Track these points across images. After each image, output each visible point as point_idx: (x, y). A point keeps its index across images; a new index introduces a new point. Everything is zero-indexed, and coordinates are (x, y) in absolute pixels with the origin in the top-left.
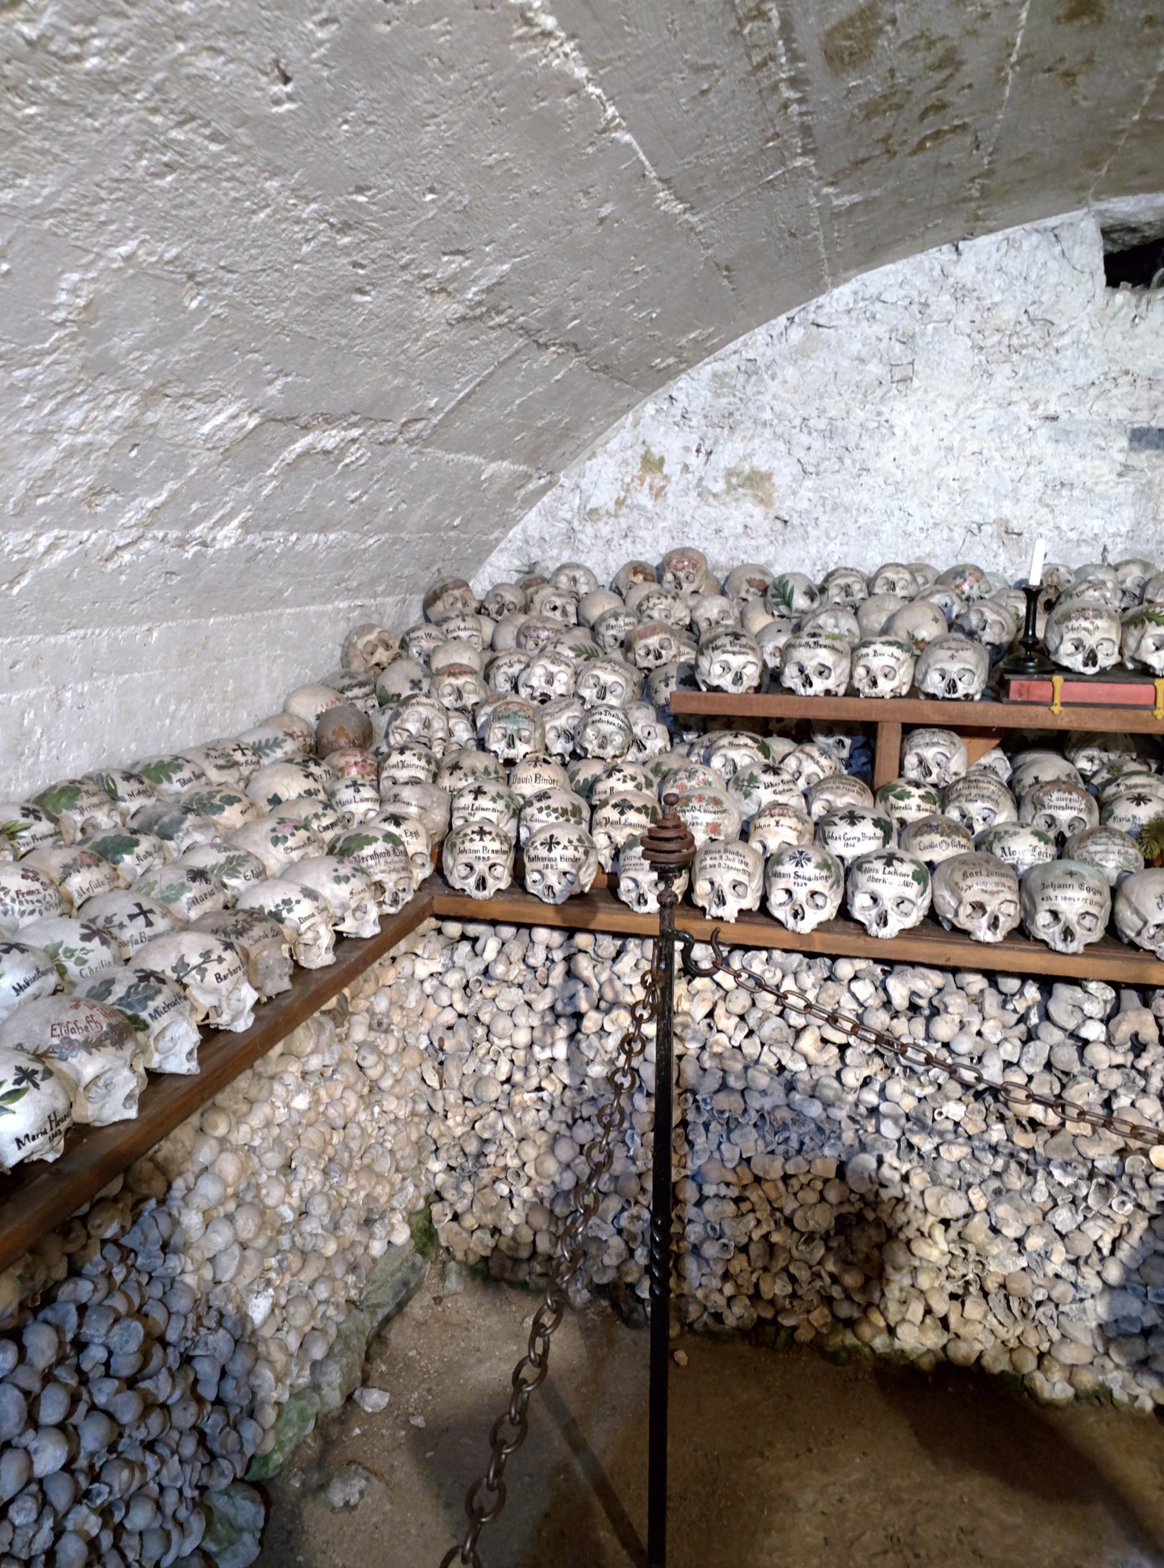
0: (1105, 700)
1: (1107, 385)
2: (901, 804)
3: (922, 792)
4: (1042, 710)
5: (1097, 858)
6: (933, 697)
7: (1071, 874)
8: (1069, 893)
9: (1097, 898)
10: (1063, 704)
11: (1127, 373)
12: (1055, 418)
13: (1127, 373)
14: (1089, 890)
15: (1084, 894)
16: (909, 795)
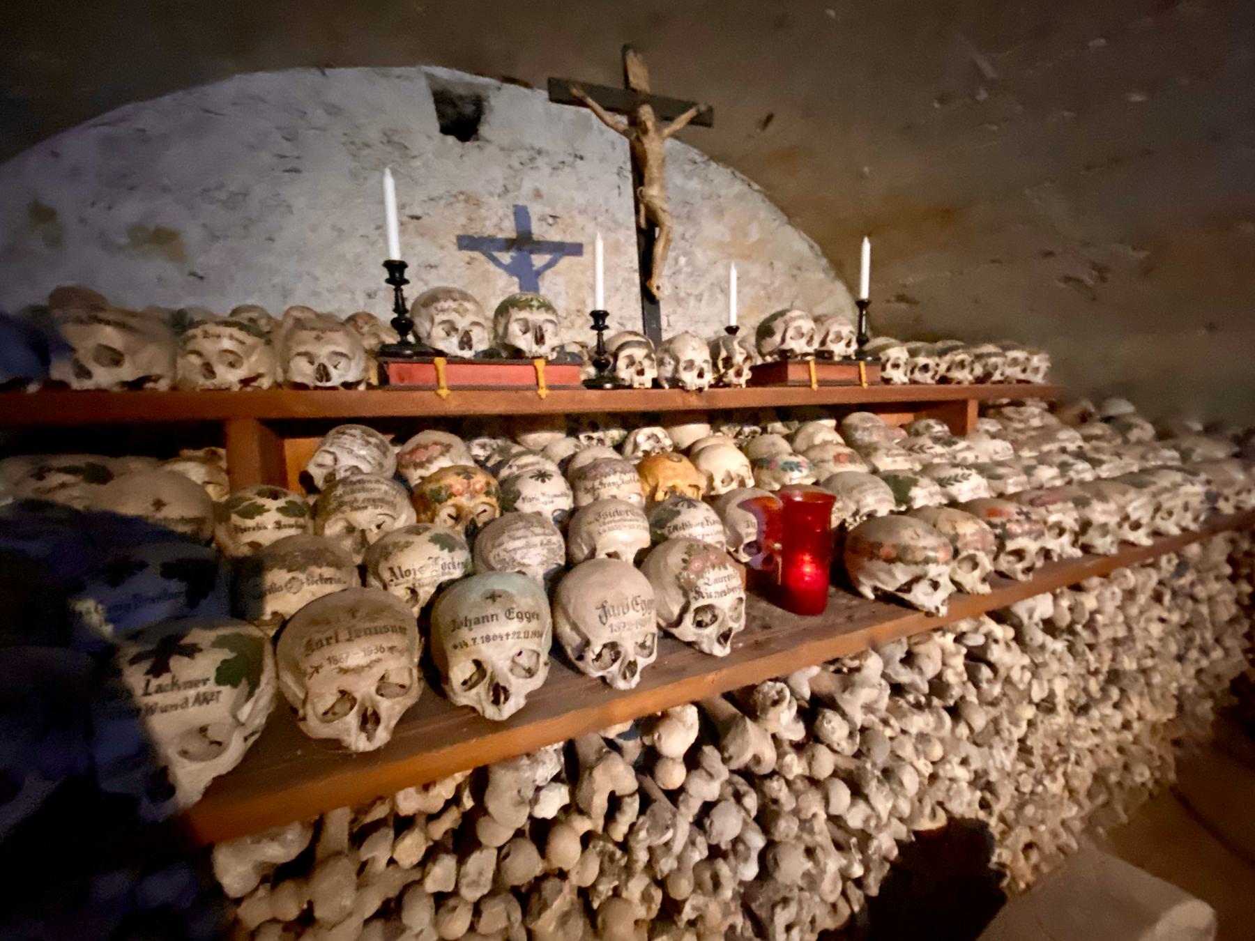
0: (492, 382)
1: (452, 199)
2: (250, 523)
3: (281, 503)
4: (427, 395)
5: (518, 556)
6: (303, 387)
7: (493, 597)
8: (495, 628)
9: (534, 625)
10: (452, 388)
11: (462, 193)
12: (418, 218)
13: (462, 193)
14: (520, 616)
15: (515, 625)
16: (261, 510)
